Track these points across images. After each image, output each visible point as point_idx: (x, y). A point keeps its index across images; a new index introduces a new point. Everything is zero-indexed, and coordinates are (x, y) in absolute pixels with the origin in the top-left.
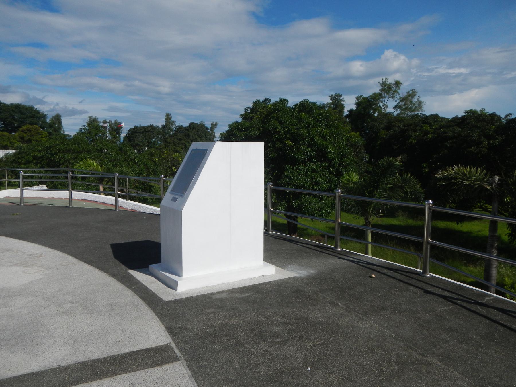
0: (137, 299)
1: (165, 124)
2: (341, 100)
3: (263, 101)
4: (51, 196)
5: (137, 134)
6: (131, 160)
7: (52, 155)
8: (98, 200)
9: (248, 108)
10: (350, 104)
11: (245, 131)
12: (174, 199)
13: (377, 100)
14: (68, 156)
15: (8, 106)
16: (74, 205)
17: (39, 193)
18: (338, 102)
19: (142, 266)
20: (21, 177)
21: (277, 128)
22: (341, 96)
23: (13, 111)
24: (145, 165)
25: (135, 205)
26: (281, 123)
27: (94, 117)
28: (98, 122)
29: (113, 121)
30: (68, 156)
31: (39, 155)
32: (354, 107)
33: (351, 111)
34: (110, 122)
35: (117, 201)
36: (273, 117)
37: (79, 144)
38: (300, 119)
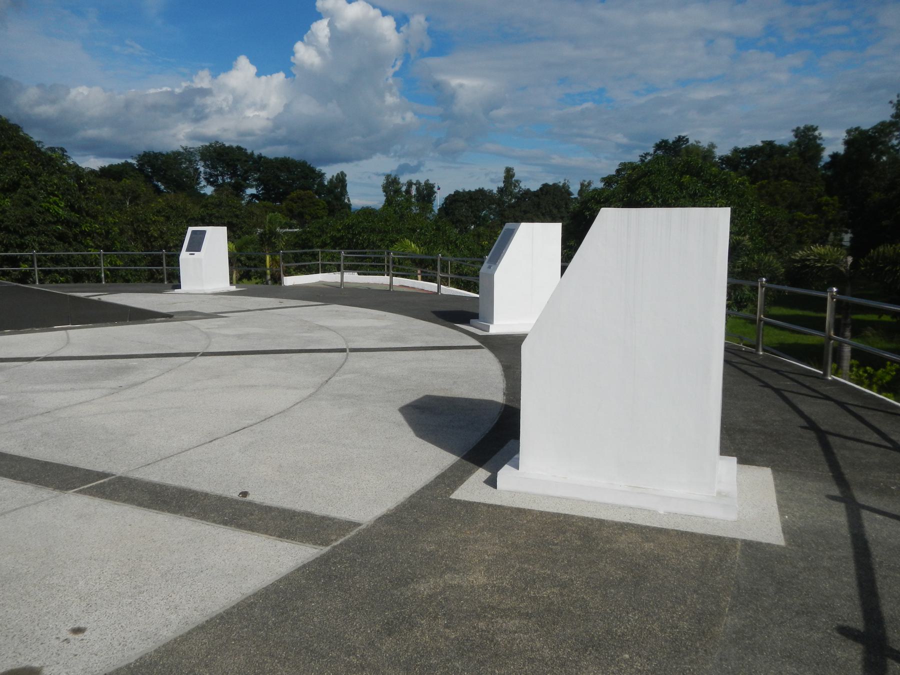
2: (815, 138)
3: (674, 142)
7: (354, 235)
9: (647, 154)
10: (833, 142)
12: (490, 267)
13: (887, 135)
14: (374, 238)
17: (352, 278)
18: (810, 140)
20: (342, 258)
21: (647, 198)
22: (815, 129)
23: (278, 168)
24: (470, 250)
26: (653, 191)
27: (393, 177)
28: (398, 183)
29: (423, 182)
30: (374, 238)
31: (338, 235)
32: (841, 149)
33: (835, 156)
34: (418, 183)
35: (439, 288)
37: (386, 221)
38: (681, 186)
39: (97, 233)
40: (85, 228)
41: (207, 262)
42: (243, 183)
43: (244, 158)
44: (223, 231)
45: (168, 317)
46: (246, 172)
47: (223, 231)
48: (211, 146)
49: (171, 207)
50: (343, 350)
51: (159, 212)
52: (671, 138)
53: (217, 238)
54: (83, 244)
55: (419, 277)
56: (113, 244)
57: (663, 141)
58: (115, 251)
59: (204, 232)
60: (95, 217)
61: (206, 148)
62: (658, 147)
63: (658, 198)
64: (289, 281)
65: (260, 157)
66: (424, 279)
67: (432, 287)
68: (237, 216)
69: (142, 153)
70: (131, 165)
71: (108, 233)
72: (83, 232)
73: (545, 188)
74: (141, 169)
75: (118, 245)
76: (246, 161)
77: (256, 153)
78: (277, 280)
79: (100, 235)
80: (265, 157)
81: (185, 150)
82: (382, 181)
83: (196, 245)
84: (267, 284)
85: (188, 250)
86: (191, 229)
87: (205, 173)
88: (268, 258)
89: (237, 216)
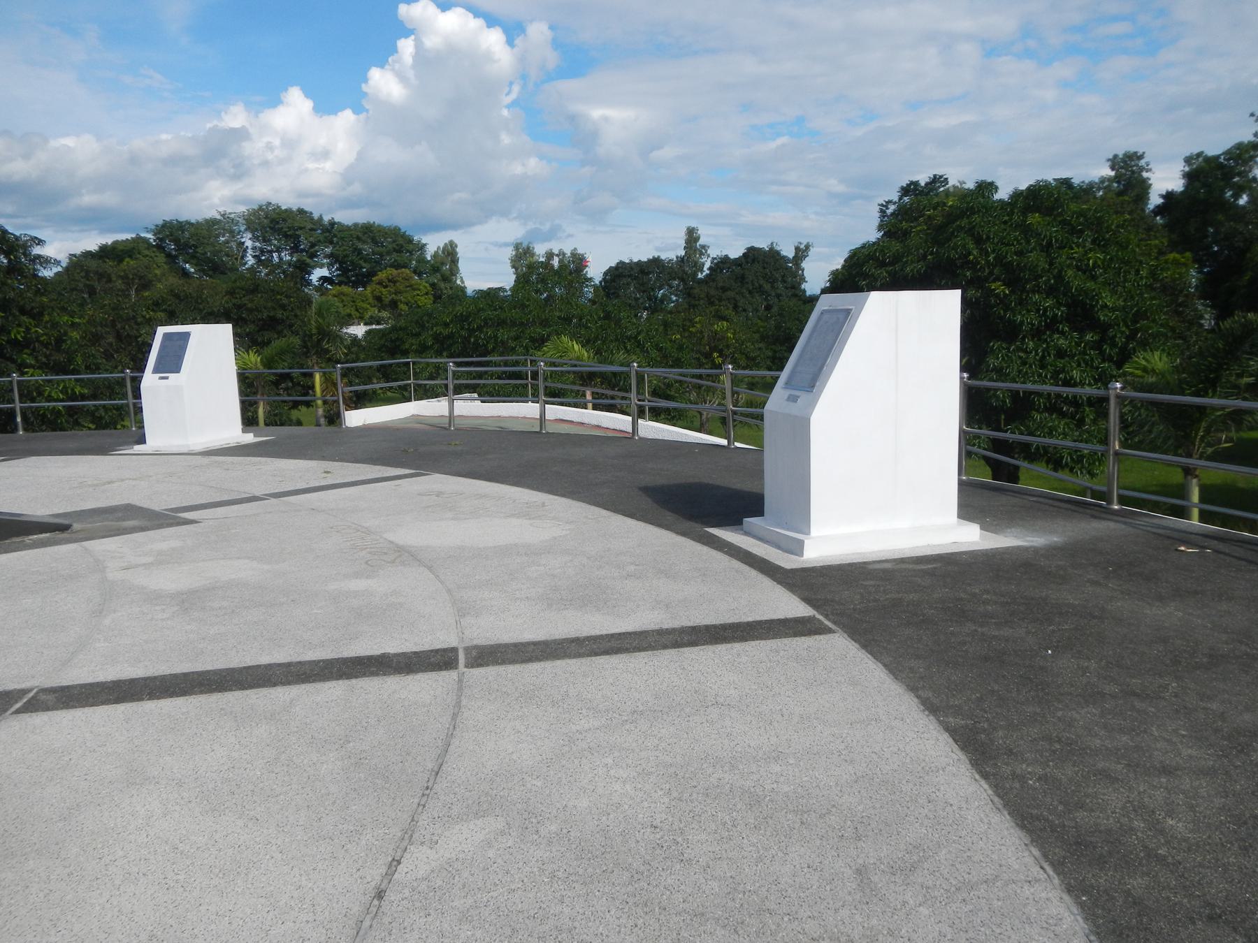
0: (736, 564)
1: (683, 253)
2: (1142, 169)
3: (927, 184)
4: (495, 414)
5: (624, 281)
6: (629, 339)
7: (471, 331)
8: (586, 421)
9: (889, 202)
11: (891, 264)
13: (1245, 162)
14: (503, 334)
15: (348, 228)
16: (550, 428)
17: (470, 408)
18: (1133, 172)
19: (733, 519)
20: (450, 375)
21: (970, 253)
22: (1141, 157)
23: (358, 238)
24: (660, 349)
25: (663, 430)
26: (979, 241)
27: (525, 245)
28: (533, 255)
30: (503, 334)
31: (446, 332)
33: (1169, 196)
36: (960, 228)
37: (523, 306)
38: (1027, 230)
39: (42, 343)
40: (18, 334)
41: (196, 387)
42: (308, 261)
43: (309, 226)
44: (223, 333)
45: (55, 529)
46: (313, 245)
47: (223, 333)
48: (260, 208)
49: (177, 296)
50: (441, 660)
51: (156, 304)
52: (923, 178)
53: (212, 349)
54: (13, 361)
55: (590, 405)
56: (70, 361)
57: (912, 183)
58: (74, 372)
59: (187, 335)
60: (37, 316)
61: (254, 213)
62: (905, 191)
63: (987, 254)
64: (355, 418)
65: (332, 223)
66: (596, 407)
67: (619, 422)
68: (283, 307)
69: (160, 222)
70: (146, 240)
71: (59, 341)
72: (14, 343)
73: (752, 255)
74: (160, 247)
75: (79, 360)
76: (312, 230)
77: (326, 218)
78: (334, 419)
79: (46, 345)
80: (339, 223)
81: (223, 215)
82: (509, 252)
83: (172, 362)
84: (318, 425)
85: (156, 371)
86: (161, 330)
87: (254, 248)
88: (317, 377)
89: (283, 307)
